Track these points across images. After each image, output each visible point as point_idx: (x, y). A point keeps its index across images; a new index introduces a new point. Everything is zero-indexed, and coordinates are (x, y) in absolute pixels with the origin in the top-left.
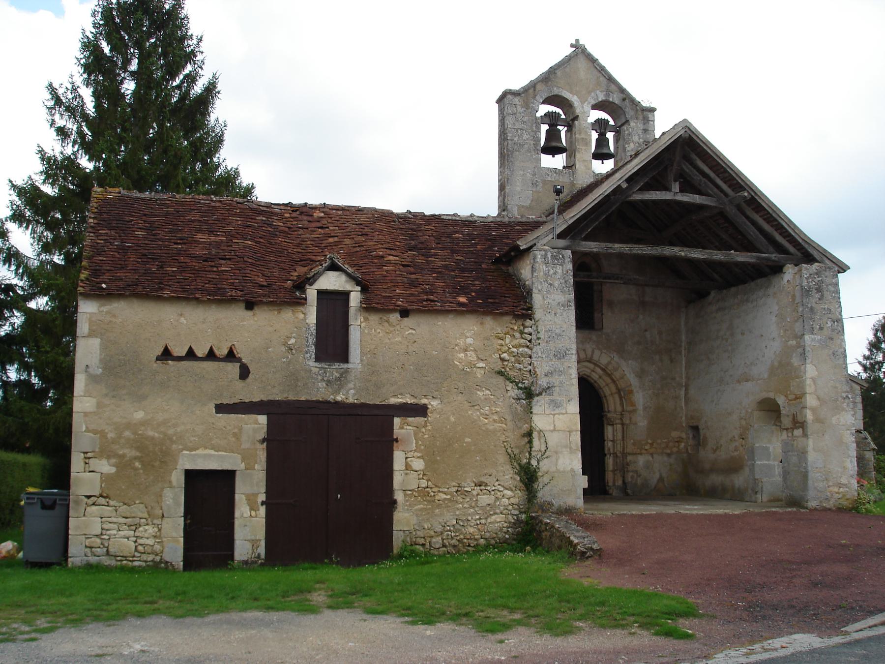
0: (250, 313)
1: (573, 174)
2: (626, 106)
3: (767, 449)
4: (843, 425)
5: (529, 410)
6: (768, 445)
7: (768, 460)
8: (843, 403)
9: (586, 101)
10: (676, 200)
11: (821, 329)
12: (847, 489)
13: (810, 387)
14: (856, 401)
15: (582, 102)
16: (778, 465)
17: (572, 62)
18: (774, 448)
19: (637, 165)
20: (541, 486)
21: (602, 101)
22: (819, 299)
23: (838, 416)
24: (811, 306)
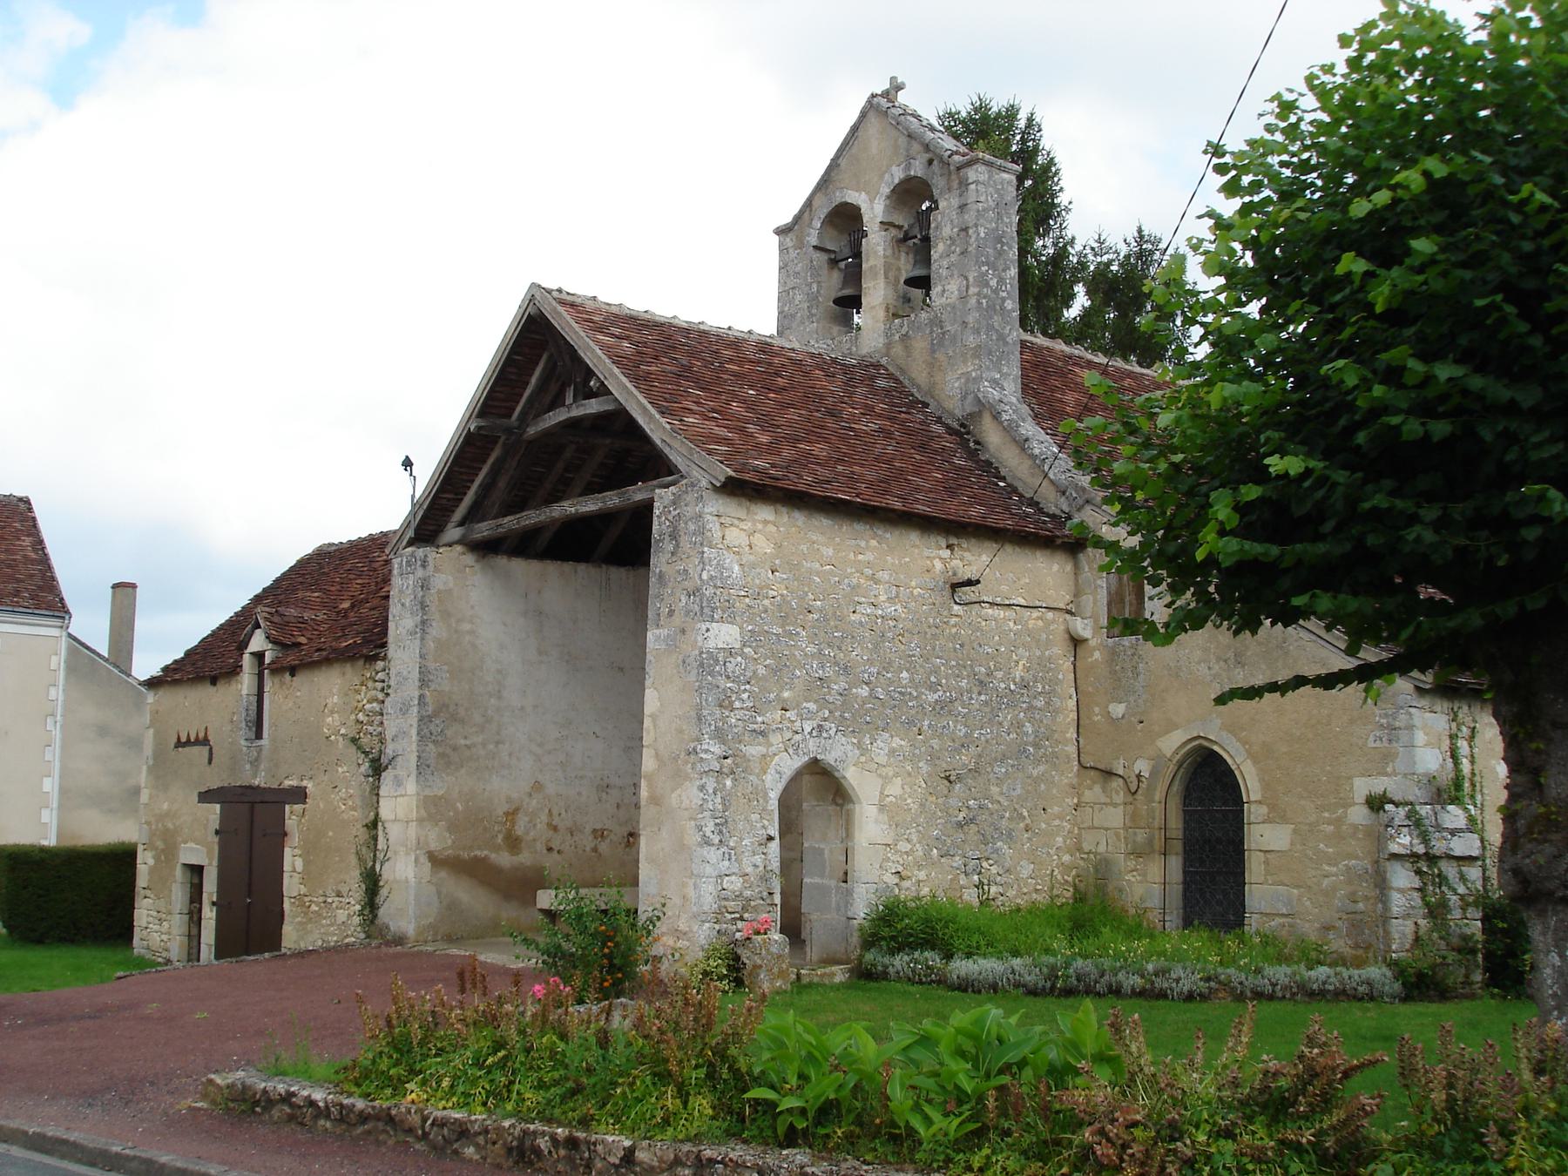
0: (215, 688)
1: (857, 339)
2: (934, 173)
3: (821, 852)
4: (686, 809)
5: (375, 791)
6: (822, 846)
7: (822, 876)
8: (686, 762)
9: (878, 193)
10: (560, 422)
11: (671, 613)
12: (688, 944)
13: (648, 733)
14: (1397, 724)
15: (872, 201)
16: (838, 888)
17: (860, 133)
18: (831, 852)
19: (485, 388)
20: (382, 899)
21: (901, 183)
22: (673, 554)
23: (679, 791)
24: (661, 571)
